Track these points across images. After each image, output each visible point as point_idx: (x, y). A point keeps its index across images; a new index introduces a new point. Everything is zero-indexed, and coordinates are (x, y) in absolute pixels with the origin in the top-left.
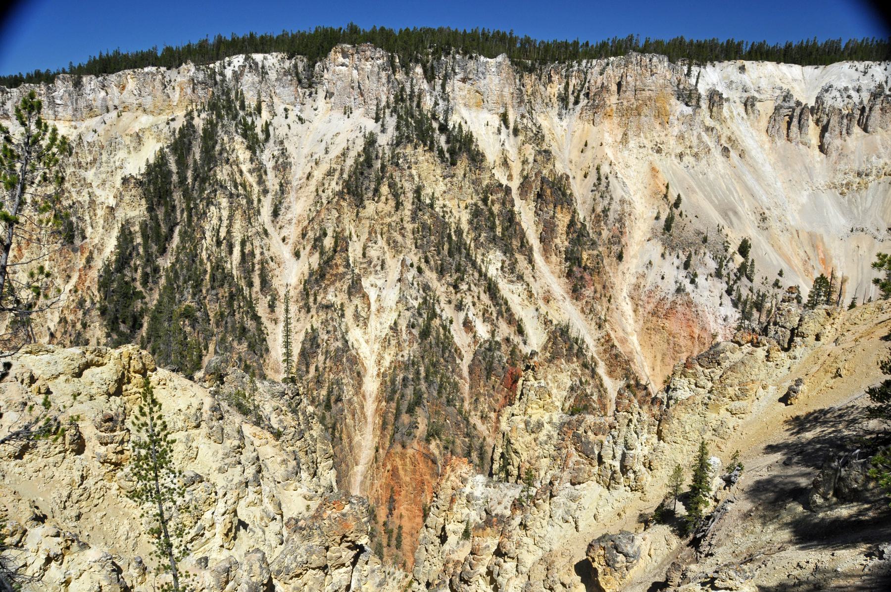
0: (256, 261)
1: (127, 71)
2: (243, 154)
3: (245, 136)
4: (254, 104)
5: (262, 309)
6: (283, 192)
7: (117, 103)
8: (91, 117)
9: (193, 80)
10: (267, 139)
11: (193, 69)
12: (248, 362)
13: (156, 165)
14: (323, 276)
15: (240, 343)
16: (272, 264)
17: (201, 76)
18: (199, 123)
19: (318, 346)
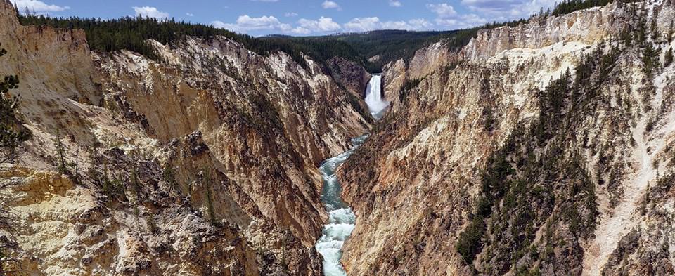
0: (612, 163)
1: (577, 12)
2: (637, 75)
3: (646, 61)
4: (664, 33)
5: (603, 203)
6: (664, 110)
7: (564, 35)
8: (547, 45)
9: (613, 16)
10: (667, 65)
11: (615, 7)
12: (564, 240)
13: (558, 82)
14: (668, 188)
15: (565, 223)
16: (627, 167)
17: (621, 12)
18: (607, 50)
19: (636, 245)
